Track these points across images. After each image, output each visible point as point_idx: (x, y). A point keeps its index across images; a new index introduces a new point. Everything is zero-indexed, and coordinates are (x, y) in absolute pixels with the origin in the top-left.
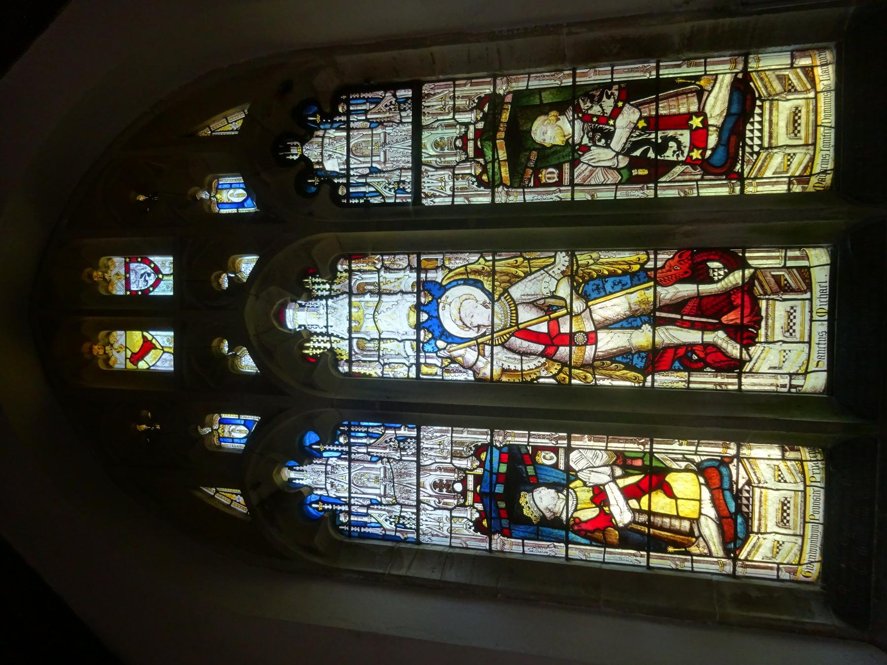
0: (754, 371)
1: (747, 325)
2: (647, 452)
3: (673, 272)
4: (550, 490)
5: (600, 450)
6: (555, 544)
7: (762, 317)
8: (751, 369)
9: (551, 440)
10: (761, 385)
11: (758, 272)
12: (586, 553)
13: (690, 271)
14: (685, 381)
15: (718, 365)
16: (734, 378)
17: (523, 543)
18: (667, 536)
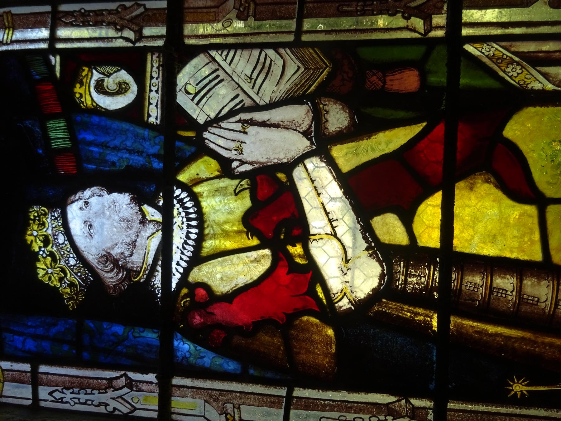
2: (437, 40)
4: (115, 195)
5: (275, 46)
6: (131, 374)
9: (121, 30)
12: (229, 406)
17: (34, 371)
18: (509, 338)
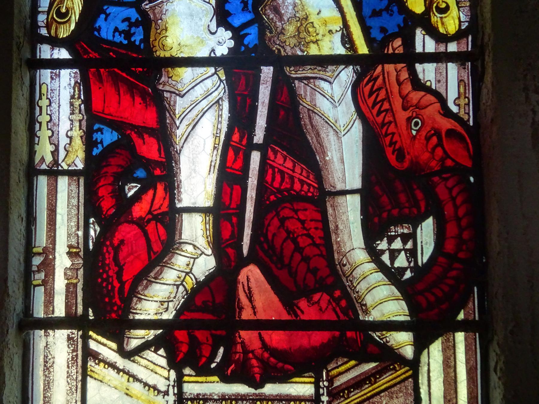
0: (91, 363)
1: (235, 344)
3: (402, 116)
7: (262, 387)
8: (95, 356)
10: (48, 386)
11: (402, 372)
13: (406, 164)
14: (56, 162)
15: (109, 259)
16: (68, 306)
